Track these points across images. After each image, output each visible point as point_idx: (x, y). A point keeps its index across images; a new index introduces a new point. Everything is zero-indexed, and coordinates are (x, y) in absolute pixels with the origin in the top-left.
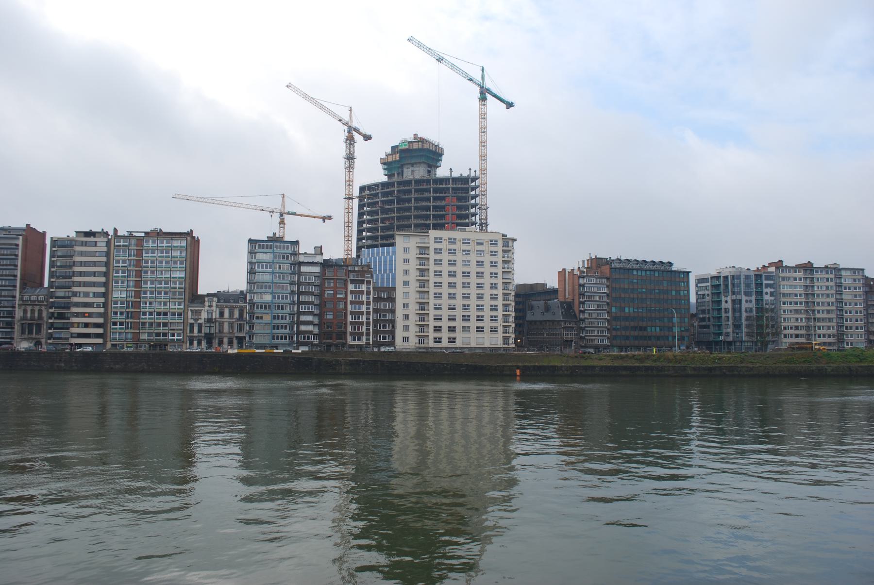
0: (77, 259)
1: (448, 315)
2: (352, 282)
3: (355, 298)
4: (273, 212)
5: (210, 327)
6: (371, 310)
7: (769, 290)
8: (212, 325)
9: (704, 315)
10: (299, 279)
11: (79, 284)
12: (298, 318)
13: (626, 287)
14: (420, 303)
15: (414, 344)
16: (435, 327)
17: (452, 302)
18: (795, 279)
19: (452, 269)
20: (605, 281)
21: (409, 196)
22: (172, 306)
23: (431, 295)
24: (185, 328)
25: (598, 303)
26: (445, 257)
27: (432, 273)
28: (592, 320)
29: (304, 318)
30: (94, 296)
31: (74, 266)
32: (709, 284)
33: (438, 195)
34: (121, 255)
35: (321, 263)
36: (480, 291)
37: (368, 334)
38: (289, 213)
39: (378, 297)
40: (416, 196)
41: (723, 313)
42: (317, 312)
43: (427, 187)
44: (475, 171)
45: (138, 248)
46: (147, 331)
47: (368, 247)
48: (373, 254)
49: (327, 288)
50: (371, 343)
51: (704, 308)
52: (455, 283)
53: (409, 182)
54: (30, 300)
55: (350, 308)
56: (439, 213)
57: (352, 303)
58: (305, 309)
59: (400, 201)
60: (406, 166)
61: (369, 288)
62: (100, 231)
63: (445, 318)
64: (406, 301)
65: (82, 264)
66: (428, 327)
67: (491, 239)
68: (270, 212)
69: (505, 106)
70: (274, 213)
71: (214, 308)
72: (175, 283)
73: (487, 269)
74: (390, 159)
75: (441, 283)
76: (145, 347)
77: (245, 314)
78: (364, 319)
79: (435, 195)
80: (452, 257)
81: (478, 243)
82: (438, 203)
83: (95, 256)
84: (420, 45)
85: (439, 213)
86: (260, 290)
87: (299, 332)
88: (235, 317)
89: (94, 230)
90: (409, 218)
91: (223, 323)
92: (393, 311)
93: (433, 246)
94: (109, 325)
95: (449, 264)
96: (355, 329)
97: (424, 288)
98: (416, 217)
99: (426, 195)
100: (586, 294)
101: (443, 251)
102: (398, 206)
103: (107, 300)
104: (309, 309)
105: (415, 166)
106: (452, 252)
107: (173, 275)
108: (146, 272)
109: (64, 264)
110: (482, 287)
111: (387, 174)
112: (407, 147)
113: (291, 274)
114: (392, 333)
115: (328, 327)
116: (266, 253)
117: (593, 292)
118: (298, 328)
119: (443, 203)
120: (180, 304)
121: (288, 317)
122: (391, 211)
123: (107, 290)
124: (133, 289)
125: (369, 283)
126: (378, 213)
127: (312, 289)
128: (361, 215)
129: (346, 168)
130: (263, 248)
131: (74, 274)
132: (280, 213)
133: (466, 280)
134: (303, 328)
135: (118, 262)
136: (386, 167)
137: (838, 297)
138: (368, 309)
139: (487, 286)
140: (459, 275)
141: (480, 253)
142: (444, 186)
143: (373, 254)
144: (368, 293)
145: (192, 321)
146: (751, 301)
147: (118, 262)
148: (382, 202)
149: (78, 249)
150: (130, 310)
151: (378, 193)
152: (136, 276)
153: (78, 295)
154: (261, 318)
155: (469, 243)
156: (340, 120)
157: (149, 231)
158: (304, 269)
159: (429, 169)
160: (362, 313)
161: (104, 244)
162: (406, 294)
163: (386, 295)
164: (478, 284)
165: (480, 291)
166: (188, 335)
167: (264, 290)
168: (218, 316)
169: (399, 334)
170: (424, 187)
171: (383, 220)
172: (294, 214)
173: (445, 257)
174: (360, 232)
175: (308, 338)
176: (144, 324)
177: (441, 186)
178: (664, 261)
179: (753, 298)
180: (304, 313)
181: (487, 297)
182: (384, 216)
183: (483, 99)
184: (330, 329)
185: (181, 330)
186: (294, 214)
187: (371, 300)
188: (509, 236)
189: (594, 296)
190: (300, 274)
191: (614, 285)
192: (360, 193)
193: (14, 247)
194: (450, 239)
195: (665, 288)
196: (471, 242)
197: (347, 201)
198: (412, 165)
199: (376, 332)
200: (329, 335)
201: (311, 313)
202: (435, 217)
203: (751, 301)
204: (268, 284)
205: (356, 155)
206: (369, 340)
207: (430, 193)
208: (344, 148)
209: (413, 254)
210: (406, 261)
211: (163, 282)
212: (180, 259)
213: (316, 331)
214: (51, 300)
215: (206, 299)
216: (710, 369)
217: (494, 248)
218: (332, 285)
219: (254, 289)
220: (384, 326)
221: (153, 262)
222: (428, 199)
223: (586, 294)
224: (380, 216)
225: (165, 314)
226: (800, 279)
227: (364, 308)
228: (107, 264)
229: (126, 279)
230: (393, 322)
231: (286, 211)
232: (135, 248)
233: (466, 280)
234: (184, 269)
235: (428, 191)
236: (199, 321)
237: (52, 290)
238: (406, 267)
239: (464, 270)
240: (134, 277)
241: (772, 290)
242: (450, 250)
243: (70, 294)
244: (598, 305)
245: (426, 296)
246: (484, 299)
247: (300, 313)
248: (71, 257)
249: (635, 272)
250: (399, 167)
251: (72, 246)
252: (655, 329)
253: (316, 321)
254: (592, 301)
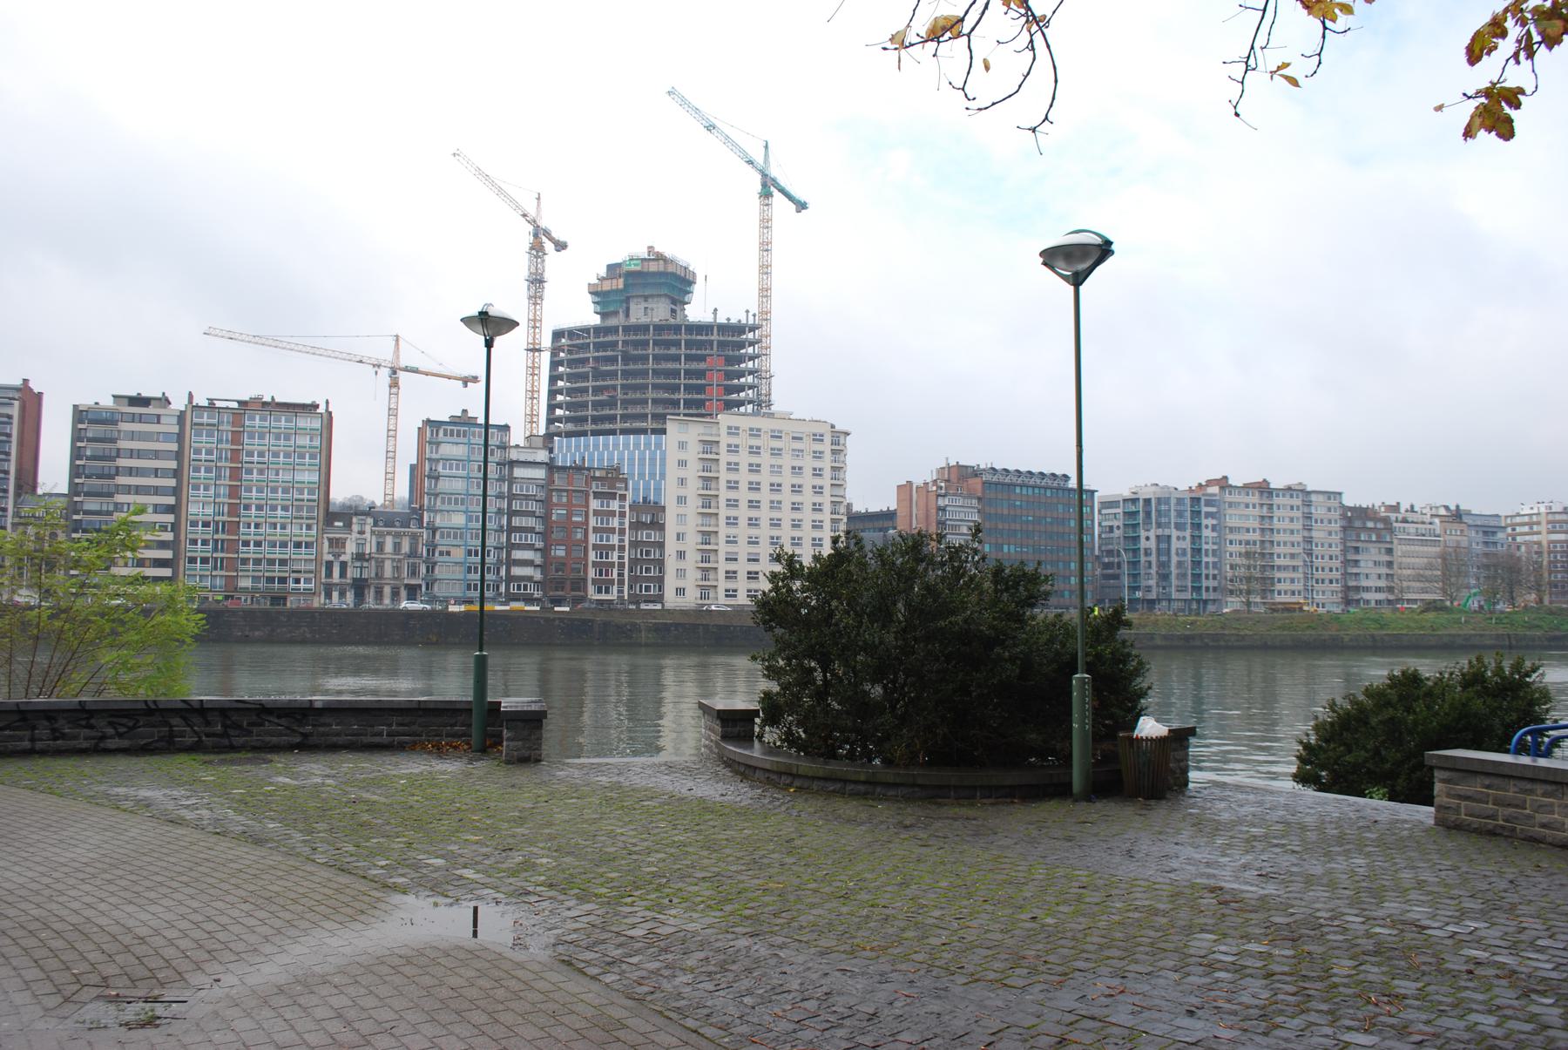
0: (124, 444)
1: (749, 554)
2: (597, 495)
3: (602, 523)
4: (379, 366)
5: (361, 568)
6: (627, 543)
7: (1210, 522)
8: (365, 564)
9: (1111, 559)
10: (510, 488)
11: (128, 490)
12: (509, 555)
13: (1006, 512)
14: (703, 533)
15: (693, 600)
16: (727, 572)
17: (753, 532)
18: (1247, 506)
19: (754, 478)
20: (975, 502)
21: (644, 352)
22: (296, 531)
23: (722, 521)
24: (318, 569)
26: (744, 459)
27: (723, 484)
29: (518, 555)
30: (155, 512)
31: (118, 456)
32: (1120, 510)
33: (694, 352)
34: (204, 441)
35: (546, 464)
36: (797, 515)
37: (621, 582)
38: (406, 369)
39: (638, 522)
40: (657, 351)
41: (1142, 556)
42: (539, 544)
43: (675, 337)
44: (754, 315)
45: (234, 429)
46: (250, 574)
47: (569, 435)
48: (569, 447)
49: (556, 505)
50: (626, 598)
51: (1110, 547)
52: (759, 502)
53: (644, 328)
54: (33, 516)
55: (592, 538)
56: (695, 382)
57: (596, 530)
58: (521, 539)
59: (627, 359)
60: (635, 300)
61: (624, 507)
62: (160, 395)
63: (743, 558)
64: (681, 529)
65: (132, 454)
66: (717, 573)
67: (815, 431)
68: (374, 366)
69: (794, 206)
70: (382, 368)
71: (368, 535)
72: (301, 491)
73: (808, 481)
74: (607, 286)
75: (737, 501)
76: (246, 600)
77: (420, 546)
78: (614, 557)
79: (688, 352)
80: (755, 460)
81: (794, 438)
82: (694, 366)
83: (158, 440)
84: (684, 102)
85: (695, 382)
86: (446, 507)
87: (510, 579)
88: (403, 552)
89: (145, 394)
90: (644, 387)
91: (383, 561)
92: (661, 545)
93: (725, 440)
94: (182, 562)
95: (750, 471)
96: (601, 575)
97: (710, 507)
98: (656, 387)
99: (673, 351)
100: (948, 522)
101: (740, 449)
102: (624, 367)
103: (178, 518)
104: (526, 539)
105: (650, 300)
106: (755, 451)
107: (297, 478)
108: (250, 472)
109: (101, 454)
110: (798, 509)
111: (599, 311)
112: (638, 268)
113: (497, 480)
114: (660, 581)
115: (557, 571)
116: (457, 444)
118: (508, 571)
119: (702, 366)
120: (309, 527)
121: (492, 553)
122: (613, 374)
123: (179, 500)
124: (227, 500)
125: (623, 498)
126: (588, 377)
127: (533, 506)
128: (553, 379)
129: (530, 298)
130: (452, 435)
131: (118, 471)
132: (391, 368)
133: (776, 497)
134: (517, 571)
135: (198, 451)
136: (597, 299)
137: (1306, 534)
138: (621, 541)
139: (808, 508)
140: (765, 488)
141: (798, 453)
142: (704, 338)
143: (569, 447)
144: (622, 515)
145: (331, 558)
146: (1184, 538)
147: (198, 451)
148: (596, 359)
149: (125, 427)
150: (220, 536)
151: (589, 344)
152: (231, 478)
153: (125, 509)
154: (448, 553)
155: (781, 437)
156: (524, 215)
157: (247, 399)
158: (518, 472)
159: (674, 307)
160: (612, 547)
161: (175, 420)
162: (681, 518)
163: (650, 516)
164: (794, 504)
165: (797, 515)
166: (323, 580)
167: (453, 507)
168: (374, 550)
169: (670, 583)
170: (670, 337)
171: (597, 390)
172: (415, 371)
173: (744, 459)
174: (551, 408)
175: (525, 589)
176: (245, 561)
177: (699, 337)
178: (1010, 468)
179: (1188, 533)
180: (520, 547)
181: (807, 525)
182: (598, 383)
183: (766, 194)
184: (560, 573)
185: (311, 572)
186: (415, 371)
187: (627, 526)
188: (838, 428)
190: (512, 480)
191: (987, 509)
192: (553, 342)
193: (6, 419)
194: (751, 429)
195: (1061, 516)
196: (783, 435)
197: (531, 354)
198: (646, 298)
199: (634, 580)
200: (559, 585)
201: (531, 547)
202: (688, 388)
203: (1184, 538)
204: (460, 497)
205: (547, 276)
206: (622, 592)
207: (680, 348)
208: (526, 263)
209: (693, 453)
210: (682, 463)
211: (280, 490)
212: (311, 450)
213: (538, 576)
214: (75, 517)
215: (355, 520)
216: (1187, 638)
217: (818, 447)
218: (565, 500)
219: (435, 504)
220: (648, 570)
221: (261, 454)
222: (677, 358)
223: (948, 522)
224: (590, 384)
225: (284, 545)
226: (1254, 506)
227: (615, 540)
228: (179, 456)
229: (213, 482)
230: (660, 563)
231: (403, 364)
232: (230, 428)
233: (776, 497)
234: (317, 468)
235: (677, 344)
236: (343, 558)
237: (76, 499)
238: (682, 473)
239: (815, 484)
240: (227, 478)
241: (1215, 522)
242: (751, 447)
243: (111, 508)
245: (713, 521)
246: (804, 527)
247: (511, 547)
248: (113, 441)
249: (1018, 490)
250: (622, 302)
251: (114, 422)
253: (538, 559)
254: (958, 534)
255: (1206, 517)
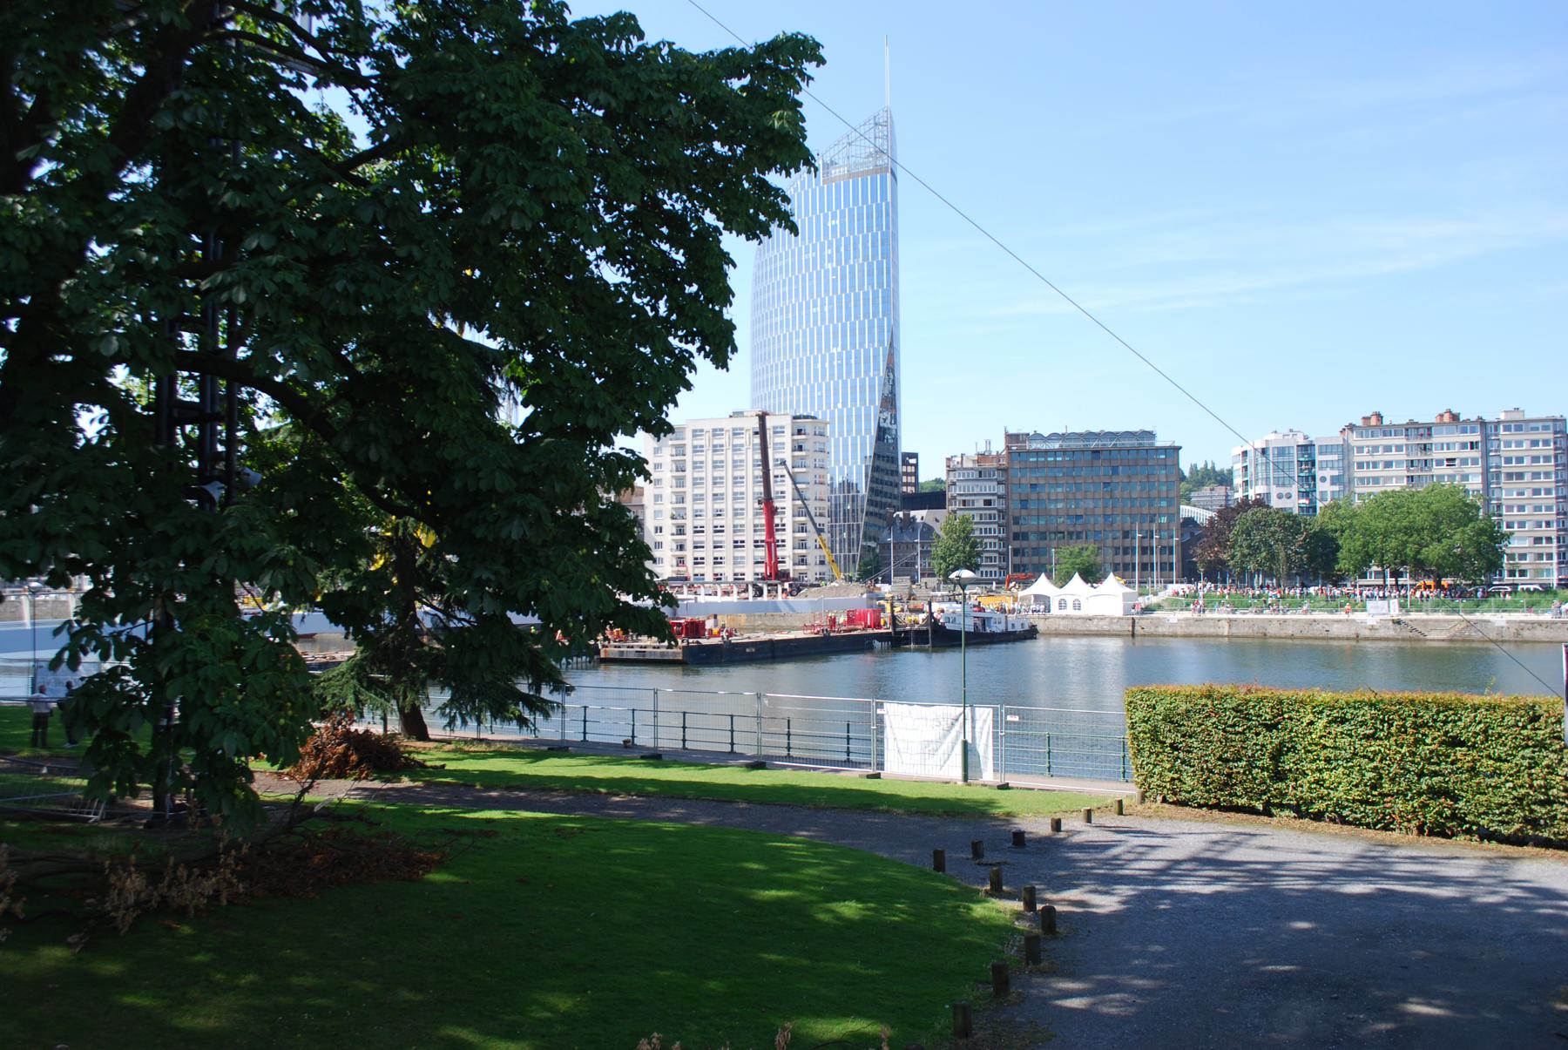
7: (1328, 473)
25: (981, 512)
26: (708, 457)
117: (971, 495)
146: (1289, 496)
173: (708, 457)
189: (973, 501)
244: (981, 515)
255: (1321, 468)
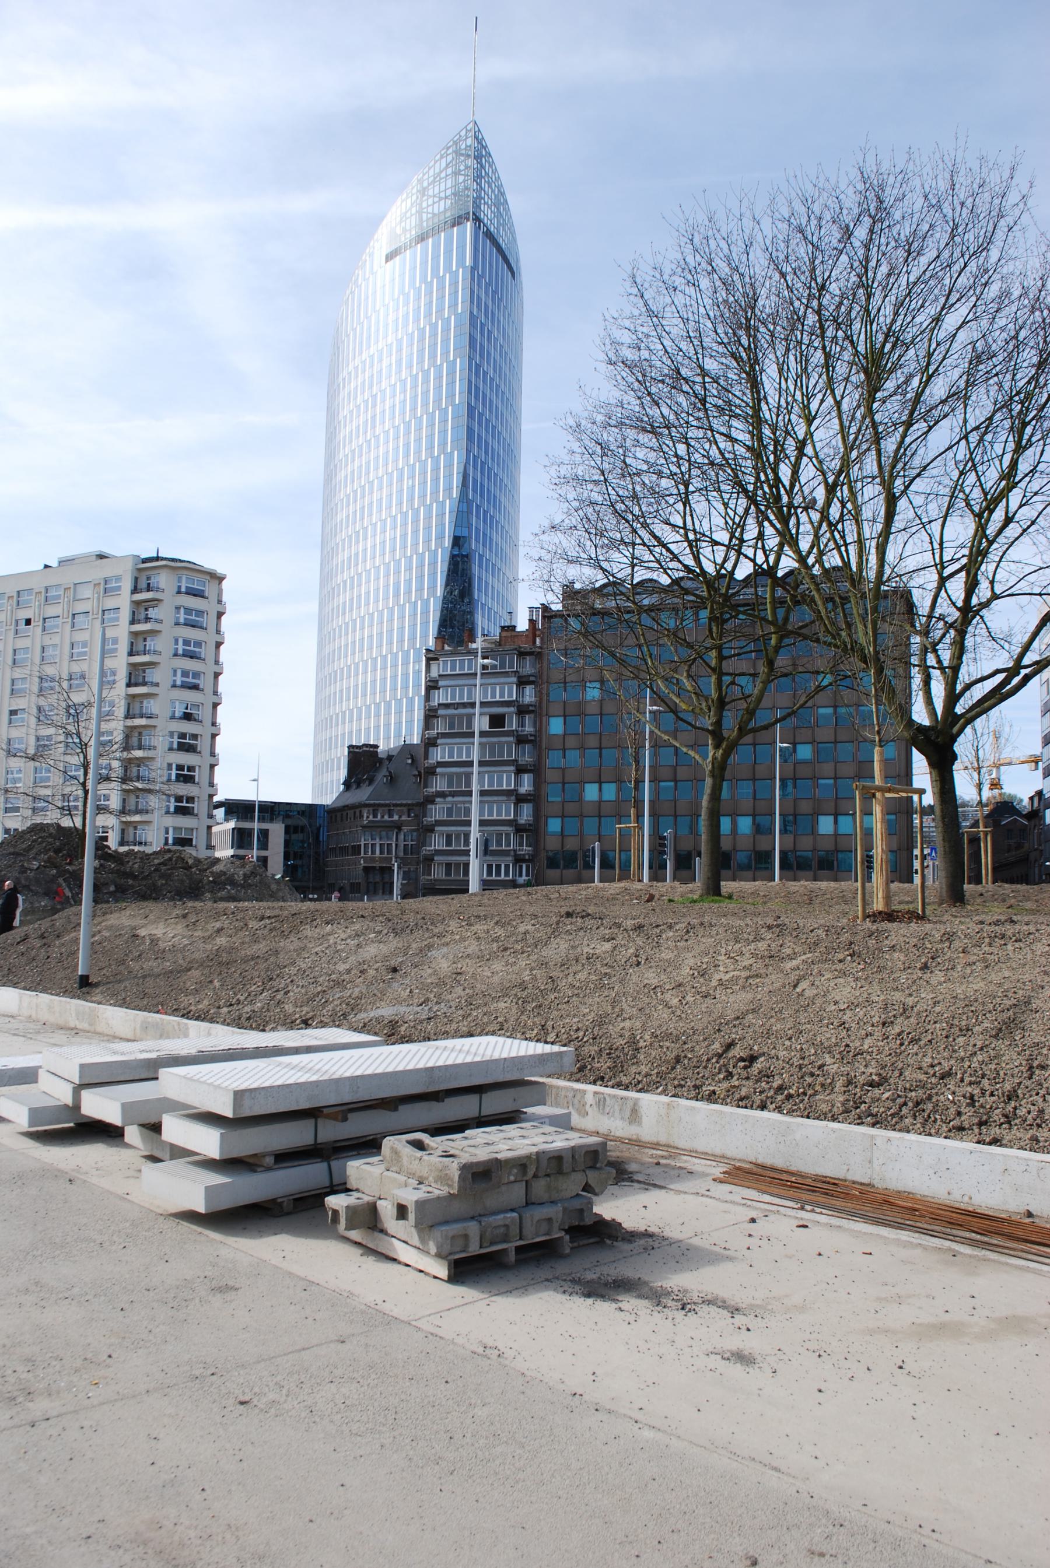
28: (456, 799)
252: (734, 824)
